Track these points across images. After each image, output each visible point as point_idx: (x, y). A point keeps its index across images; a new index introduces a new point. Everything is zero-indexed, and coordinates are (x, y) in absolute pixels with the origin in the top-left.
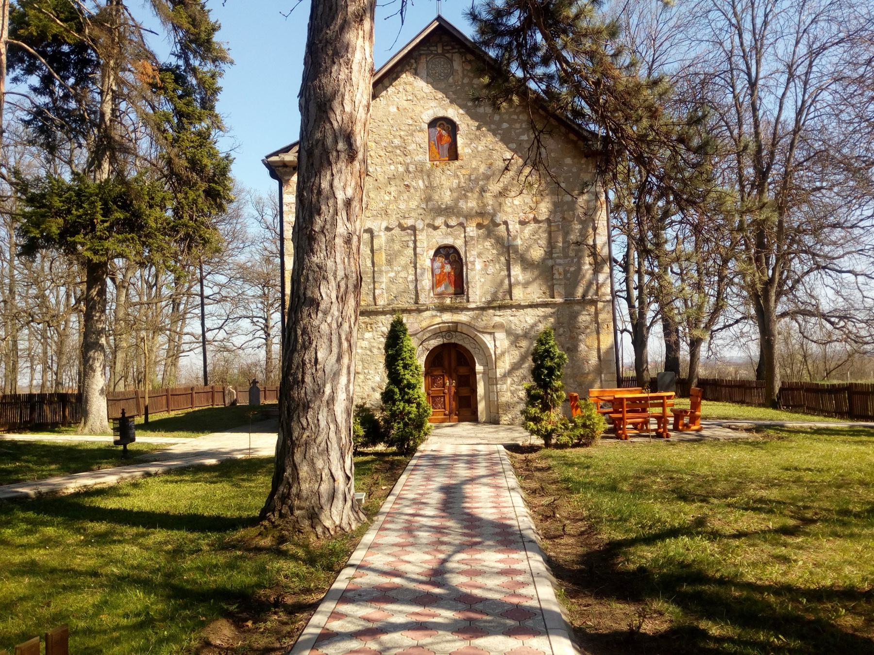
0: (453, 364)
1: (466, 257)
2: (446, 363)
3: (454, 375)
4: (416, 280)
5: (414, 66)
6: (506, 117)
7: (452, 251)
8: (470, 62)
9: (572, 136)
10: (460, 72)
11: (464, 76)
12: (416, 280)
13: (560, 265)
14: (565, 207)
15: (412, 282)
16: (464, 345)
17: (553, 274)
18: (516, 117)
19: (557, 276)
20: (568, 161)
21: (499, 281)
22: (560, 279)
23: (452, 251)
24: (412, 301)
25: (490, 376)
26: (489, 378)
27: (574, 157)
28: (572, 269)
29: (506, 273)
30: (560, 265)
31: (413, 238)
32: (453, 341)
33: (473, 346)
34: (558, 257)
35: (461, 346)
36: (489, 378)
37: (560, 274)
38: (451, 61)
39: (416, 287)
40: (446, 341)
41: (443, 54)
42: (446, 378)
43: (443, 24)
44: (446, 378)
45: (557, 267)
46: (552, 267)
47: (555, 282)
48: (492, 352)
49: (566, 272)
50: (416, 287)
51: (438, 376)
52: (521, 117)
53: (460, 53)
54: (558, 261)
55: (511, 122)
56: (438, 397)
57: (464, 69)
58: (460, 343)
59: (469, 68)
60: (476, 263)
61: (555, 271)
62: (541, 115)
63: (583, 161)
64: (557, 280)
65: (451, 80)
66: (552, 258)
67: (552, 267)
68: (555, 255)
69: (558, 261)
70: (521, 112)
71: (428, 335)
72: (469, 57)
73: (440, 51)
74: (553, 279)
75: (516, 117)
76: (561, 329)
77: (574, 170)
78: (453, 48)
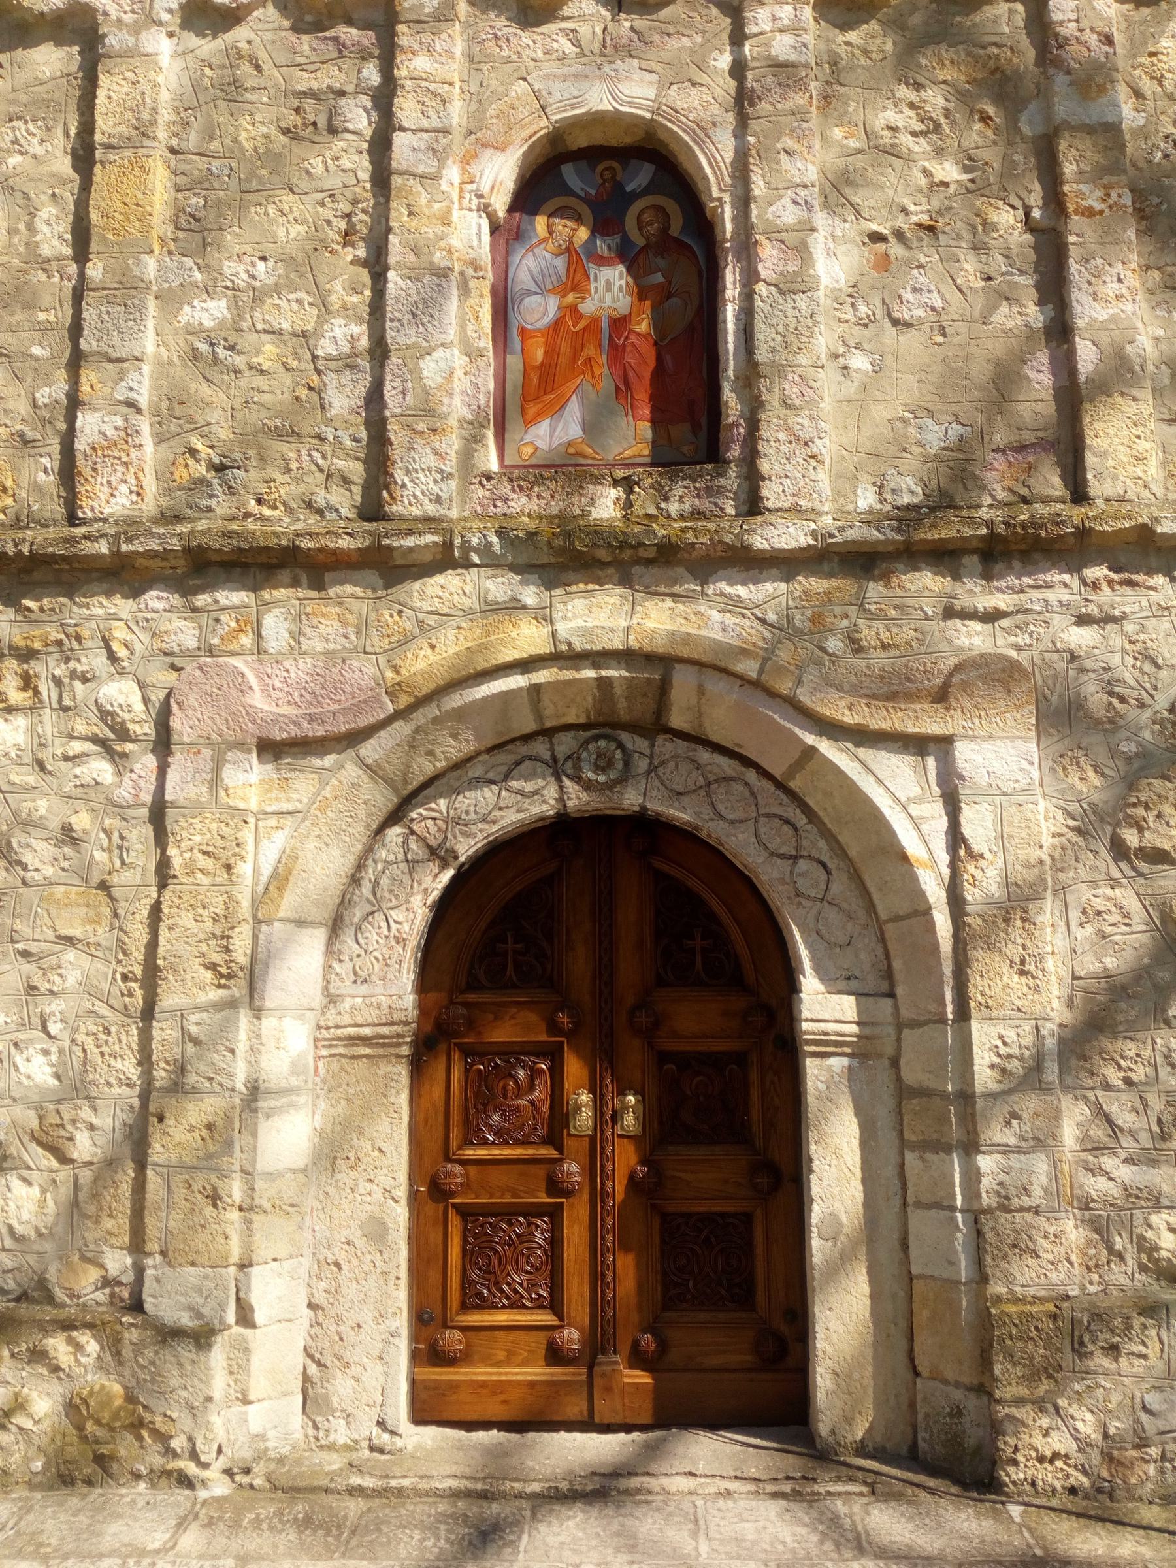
1: (744, 201)
3: (634, 1053)
4: (379, 351)
7: (641, 176)
12: (379, 351)
15: (348, 363)
16: (714, 830)
21: (981, 371)
23: (641, 176)
24: (344, 501)
25: (912, 1075)
26: (903, 1092)
29: (1034, 314)
32: (631, 799)
33: (782, 840)
35: (688, 837)
36: (903, 1092)
39: (375, 398)
40: (577, 799)
42: (574, 1068)
44: (574, 1068)
48: (935, 891)
50: (375, 398)
51: (513, 1052)
56: (508, 1213)
58: (681, 814)
60: (818, 244)
71: (451, 748)
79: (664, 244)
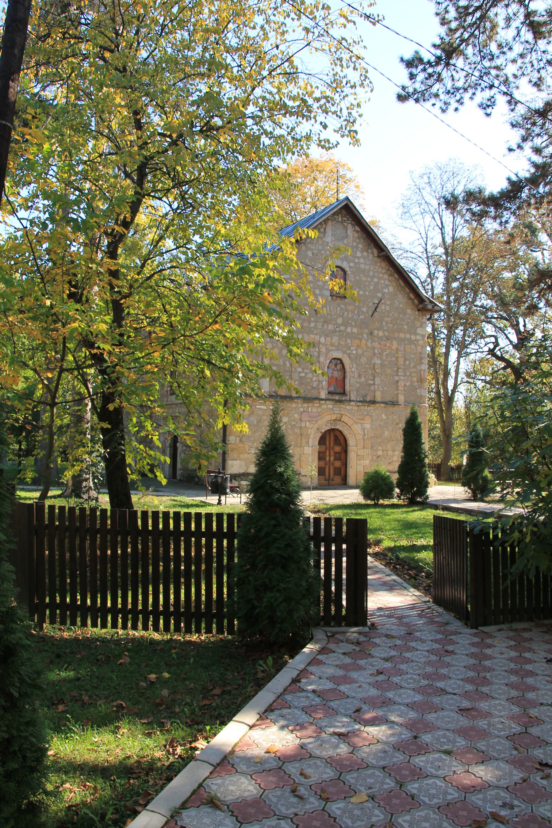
0: (332, 444)
2: (328, 443)
5: (324, 226)
6: (376, 274)
7: (339, 362)
8: (357, 232)
9: (412, 296)
10: (351, 237)
11: (353, 241)
14: (406, 342)
18: (381, 276)
19: (400, 388)
20: (409, 311)
23: (339, 362)
26: (357, 455)
27: (412, 310)
28: (408, 384)
31: (317, 349)
32: (337, 427)
34: (402, 375)
38: (346, 228)
41: (342, 222)
43: (349, 203)
46: (397, 381)
49: (405, 385)
52: (385, 276)
53: (352, 224)
55: (380, 278)
57: (354, 236)
59: (356, 235)
61: (399, 384)
62: (395, 278)
63: (417, 313)
65: (345, 241)
66: (398, 375)
67: (397, 381)
68: (400, 374)
70: (385, 273)
72: (357, 228)
73: (340, 220)
74: (397, 389)
75: (381, 276)
77: (412, 318)
78: (348, 220)
79: (341, 369)
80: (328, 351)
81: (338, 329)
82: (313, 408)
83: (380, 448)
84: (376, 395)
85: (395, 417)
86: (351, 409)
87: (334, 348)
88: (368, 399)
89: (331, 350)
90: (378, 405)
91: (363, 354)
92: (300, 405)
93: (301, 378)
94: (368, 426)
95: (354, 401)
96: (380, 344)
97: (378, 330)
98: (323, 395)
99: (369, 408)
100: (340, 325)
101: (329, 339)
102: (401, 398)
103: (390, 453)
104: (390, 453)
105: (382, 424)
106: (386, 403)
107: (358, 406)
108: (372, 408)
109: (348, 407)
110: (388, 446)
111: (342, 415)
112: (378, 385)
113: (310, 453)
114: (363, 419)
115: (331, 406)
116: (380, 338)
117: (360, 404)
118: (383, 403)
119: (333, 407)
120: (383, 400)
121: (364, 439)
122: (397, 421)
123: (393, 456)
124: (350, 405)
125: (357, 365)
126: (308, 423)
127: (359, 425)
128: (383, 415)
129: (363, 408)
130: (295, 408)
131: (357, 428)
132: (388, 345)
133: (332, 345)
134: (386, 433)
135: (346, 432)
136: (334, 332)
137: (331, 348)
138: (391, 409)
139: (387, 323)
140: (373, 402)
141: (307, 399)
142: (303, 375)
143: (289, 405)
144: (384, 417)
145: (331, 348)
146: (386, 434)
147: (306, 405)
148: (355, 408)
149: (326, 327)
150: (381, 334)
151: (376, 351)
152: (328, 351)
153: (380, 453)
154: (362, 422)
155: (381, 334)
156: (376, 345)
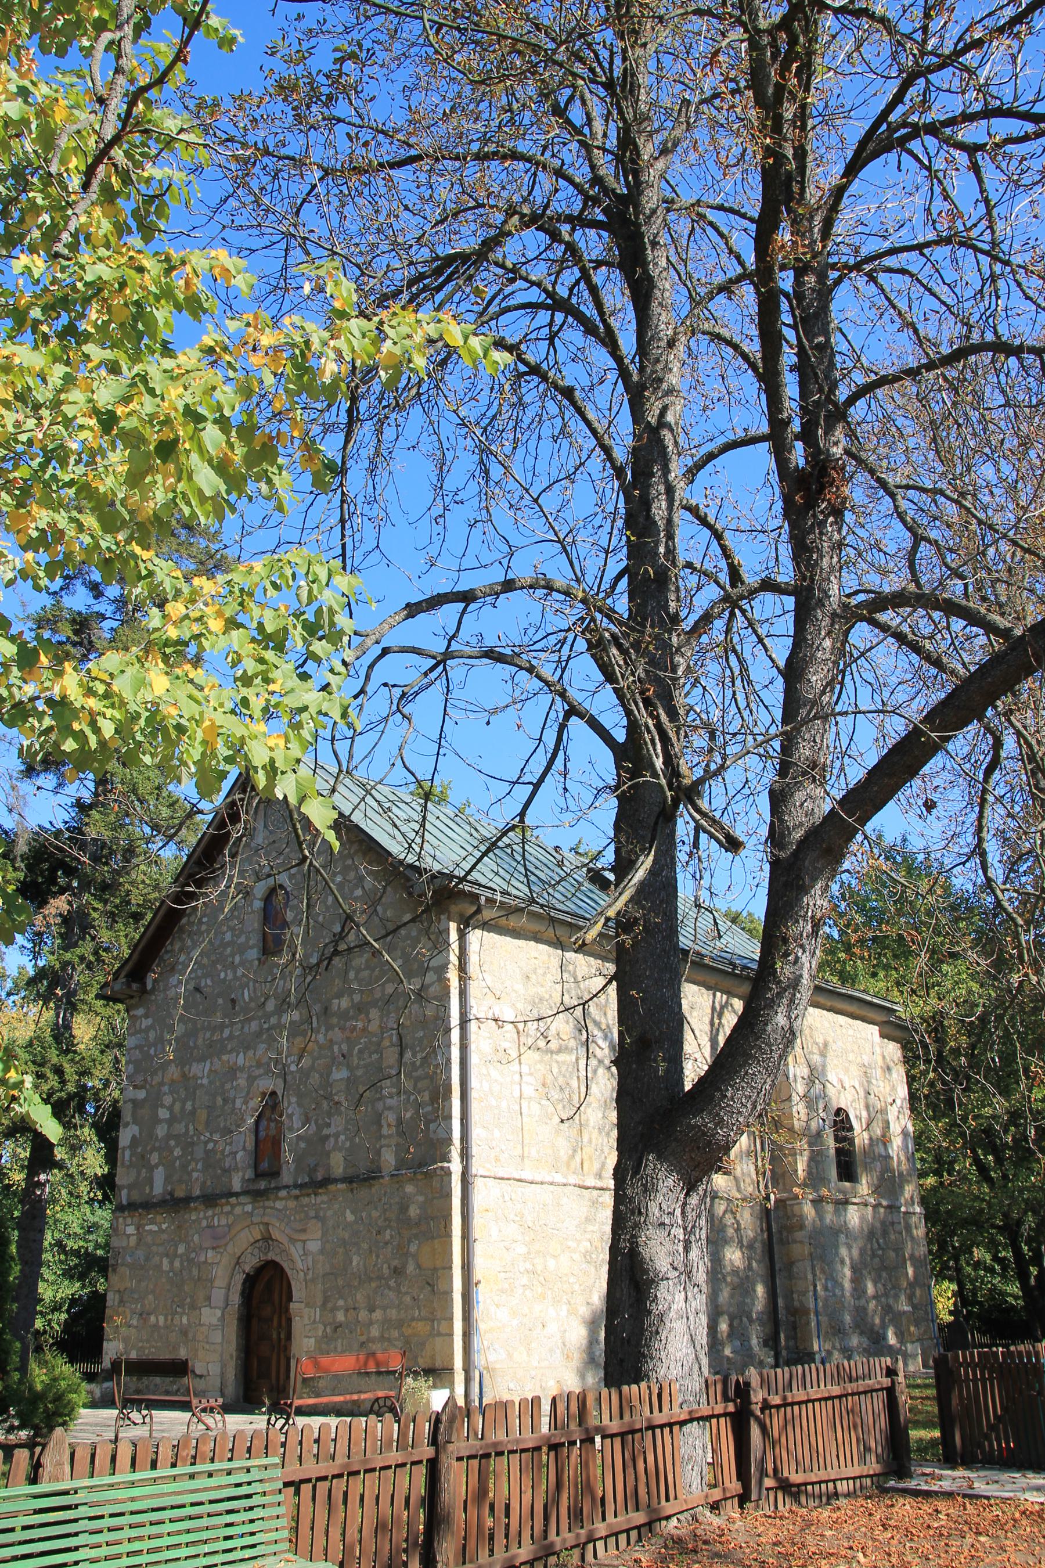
13: (390, 1108)
16: (282, 1263)
17: (380, 1126)
19: (385, 1131)
22: (390, 1136)
30: (390, 1108)
37: (389, 1125)
45: (386, 1112)
47: (383, 1142)
49: (400, 1121)
54: (389, 1102)
61: (383, 1122)
64: (385, 1137)
69: (389, 1102)
76: (388, 1232)
80: (251, 1080)
81: (266, 1026)
82: (219, 1218)
83: (341, 1303)
84: (333, 1162)
85: (375, 1214)
86: (286, 1208)
87: (262, 1071)
88: (319, 1176)
89: (256, 1078)
90: (332, 1187)
91: (312, 1067)
92: (202, 1215)
93: (207, 1152)
94: (314, 1246)
95: (287, 1187)
96: (342, 1029)
97: (339, 996)
98: (237, 1186)
99: (319, 1199)
100: (272, 1014)
101: (250, 1053)
102: (389, 1158)
103: (363, 1315)
104: (363, 1315)
105: (347, 1236)
106: (349, 1180)
107: (297, 1197)
108: (325, 1198)
109: (279, 1205)
110: (359, 1296)
111: (267, 1224)
112: (337, 1136)
113: (214, 1321)
114: (304, 1231)
115: (249, 1208)
116: (344, 1015)
117: (296, 1192)
118: (343, 1180)
119: (254, 1209)
120: (351, 1172)
121: (305, 1280)
122: (380, 1222)
123: (371, 1323)
124: (277, 1198)
125: (300, 1096)
126: (210, 1253)
127: (299, 1245)
128: (348, 1213)
129: (305, 1200)
130: (194, 1221)
131: (295, 1252)
132: (360, 1025)
133: (259, 1065)
134: (355, 1260)
135: (285, 1265)
136: (259, 1034)
137: (257, 1072)
138: (363, 1193)
139: (358, 971)
140: (327, 1181)
141: (210, 1200)
142: (210, 1146)
143: (187, 1216)
144: (350, 1217)
145: (257, 1072)
146: (354, 1263)
147: (210, 1213)
148: (292, 1204)
149: (246, 1030)
150: (344, 1003)
151: (336, 1048)
152: (251, 1080)
153: (340, 1317)
154: (304, 1237)
155: (344, 1003)
156: (337, 1034)
